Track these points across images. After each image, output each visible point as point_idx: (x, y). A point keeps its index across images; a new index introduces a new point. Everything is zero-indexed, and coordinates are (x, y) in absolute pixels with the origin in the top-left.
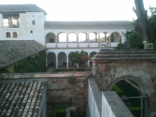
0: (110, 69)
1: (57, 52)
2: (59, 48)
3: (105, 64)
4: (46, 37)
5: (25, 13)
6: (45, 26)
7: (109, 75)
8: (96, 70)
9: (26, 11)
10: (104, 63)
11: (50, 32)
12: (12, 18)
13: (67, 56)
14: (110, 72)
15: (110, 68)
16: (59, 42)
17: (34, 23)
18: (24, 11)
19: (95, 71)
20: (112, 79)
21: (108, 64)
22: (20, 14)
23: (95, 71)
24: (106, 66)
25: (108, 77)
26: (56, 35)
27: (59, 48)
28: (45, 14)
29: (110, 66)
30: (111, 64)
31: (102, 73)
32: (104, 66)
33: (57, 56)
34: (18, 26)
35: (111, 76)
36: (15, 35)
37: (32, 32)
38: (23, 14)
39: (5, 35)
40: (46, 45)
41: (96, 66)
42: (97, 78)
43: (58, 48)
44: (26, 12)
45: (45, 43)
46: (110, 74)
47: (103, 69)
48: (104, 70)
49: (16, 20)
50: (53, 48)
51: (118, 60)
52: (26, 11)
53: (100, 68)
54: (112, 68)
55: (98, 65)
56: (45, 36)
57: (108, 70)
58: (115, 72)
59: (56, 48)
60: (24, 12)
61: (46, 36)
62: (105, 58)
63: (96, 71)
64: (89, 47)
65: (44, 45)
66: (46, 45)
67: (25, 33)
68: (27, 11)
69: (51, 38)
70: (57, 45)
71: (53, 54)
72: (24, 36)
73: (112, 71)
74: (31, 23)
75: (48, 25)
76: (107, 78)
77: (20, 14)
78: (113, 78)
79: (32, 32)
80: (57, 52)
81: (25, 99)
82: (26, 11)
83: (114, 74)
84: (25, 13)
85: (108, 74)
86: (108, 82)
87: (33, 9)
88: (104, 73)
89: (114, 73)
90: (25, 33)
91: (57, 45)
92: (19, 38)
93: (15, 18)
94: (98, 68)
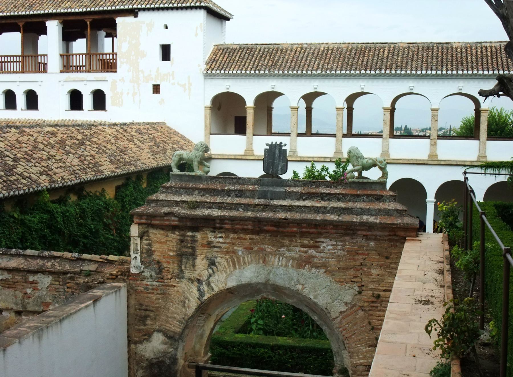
0: (193, 255)
3: (177, 233)
4: (209, 111)
5: (136, 15)
6: (207, 64)
8: (142, 253)
10: (173, 228)
12: (103, 33)
14: (194, 266)
15: (193, 249)
17: (166, 52)
18: (131, 7)
19: (136, 257)
20: (201, 293)
21: (189, 234)
22: (120, 21)
23: (138, 256)
24: (182, 241)
26: (250, 103)
29: (194, 240)
30: (199, 236)
32: (174, 236)
34: (109, 66)
35: (199, 281)
36: (99, 100)
37: (156, 89)
41: (141, 237)
42: (145, 282)
45: (206, 136)
46: (196, 275)
48: (171, 254)
51: (222, 219)
52: (139, 6)
55: (151, 235)
57: (186, 254)
58: (215, 268)
60: (133, 12)
61: (208, 104)
62: (176, 209)
63: (141, 256)
64: (432, 162)
68: (144, 9)
72: (129, 103)
73: (201, 262)
75: (225, 59)
76: (183, 285)
77: (120, 21)
79: (156, 89)
82: (140, 9)
84: (136, 16)
85: (187, 274)
89: (210, 271)
94: (150, 245)
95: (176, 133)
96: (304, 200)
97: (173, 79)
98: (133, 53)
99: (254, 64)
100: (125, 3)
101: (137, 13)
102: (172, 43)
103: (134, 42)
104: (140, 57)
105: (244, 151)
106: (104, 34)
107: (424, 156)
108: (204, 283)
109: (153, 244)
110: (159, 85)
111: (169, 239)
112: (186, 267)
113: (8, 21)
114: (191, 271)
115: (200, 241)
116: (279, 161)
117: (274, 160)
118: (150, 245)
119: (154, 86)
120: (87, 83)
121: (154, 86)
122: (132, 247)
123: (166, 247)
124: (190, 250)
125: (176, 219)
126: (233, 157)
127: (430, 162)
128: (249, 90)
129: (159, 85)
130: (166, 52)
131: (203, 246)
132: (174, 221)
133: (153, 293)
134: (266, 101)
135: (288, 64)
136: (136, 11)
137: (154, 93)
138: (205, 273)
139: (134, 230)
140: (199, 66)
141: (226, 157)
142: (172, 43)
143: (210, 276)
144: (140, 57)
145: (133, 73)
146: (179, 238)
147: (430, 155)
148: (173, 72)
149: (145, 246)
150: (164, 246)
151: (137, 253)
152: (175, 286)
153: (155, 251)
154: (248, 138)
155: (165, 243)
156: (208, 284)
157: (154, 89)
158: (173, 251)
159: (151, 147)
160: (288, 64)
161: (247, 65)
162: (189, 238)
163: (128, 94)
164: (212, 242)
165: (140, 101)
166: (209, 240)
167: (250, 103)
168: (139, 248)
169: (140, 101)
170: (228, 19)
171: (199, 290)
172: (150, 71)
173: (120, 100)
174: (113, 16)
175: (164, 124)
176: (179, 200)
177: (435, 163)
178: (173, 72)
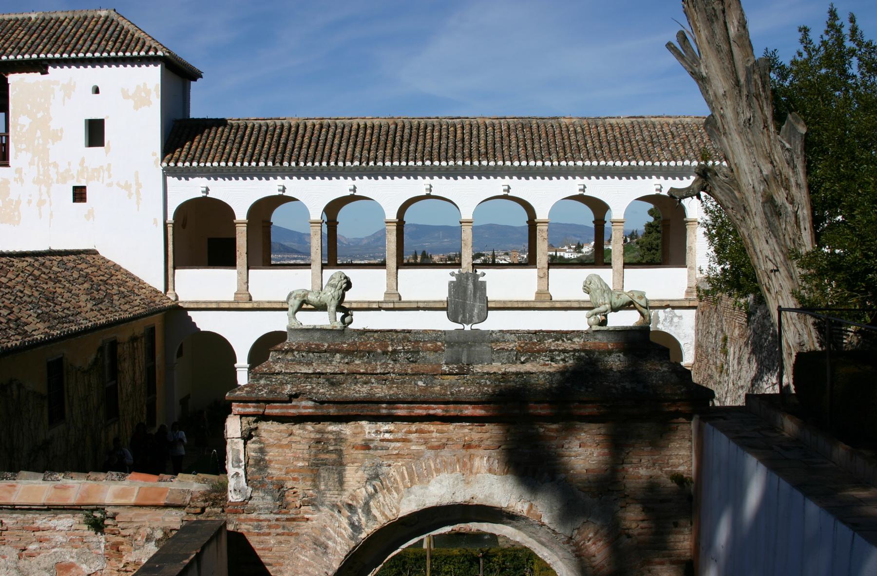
0: (339, 465)
5: (44, 72)
7: (338, 500)
11: (201, 195)
14: (341, 482)
15: (340, 453)
17: (95, 132)
19: (237, 474)
20: (356, 528)
23: (242, 472)
24: (318, 442)
25: (325, 509)
26: (241, 215)
29: (340, 439)
31: (289, 484)
37: (79, 194)
42: (253, 515)
44: (50, 69)
46: (345, 498)
47: (298, 459)
48: (300, 464)
53: (272, 454)
54: (350, 454)
55: (263, 434)
57: (327, 462)
58: (376, 483)
60: (40, 67)
67: (41, 203)
74: (81, 133)
78: (363, 520)
79: (79, 194)
83: (371, 496)
85: (331, 496)
86: (330, 543)
88: (302, 487)
90: (41, 203)
94: (262, 451)
95: (117, 268)
96: (522, 363)
97: (110, 177)
98: (39, 134)
99: (246, 151)
100: (23, 50)
102: (107, 117)
103: (39, 115)
104: (50, 141)
105: (233, 296)
107: (529, 294)
108: (360, 511)
109: (267, 449)
110: (84, 187)
111: (294, 438)
112: (326, 485)
114: (336, 492)
115: (351, 440)
116: (475, 301)
117: (465, 300)
118: (262, 451)
119: (75, 188)
121: (75, 188)
122: (230, 456)
123: (289, 454)
124: (334, 456)
125: (311, 403)
126: (214, 306)
127: (539, 305)
128: (240, 195)
129: (84, 187)
130: (95, 132)
131: (355, 447)
132: (305, 407)
133: (269, 534)
134: (263, 210)
135: (304, 151)
136: (46, 63)
137: (74, 201)
138: (362, 493)
139: (233, 427)
140: (154, 154)
141: (203, 306)
142: (107, 117)
143: (371, 496)
144: (50, 141)
145: (38, 166)
146: (313, 436)
147: (538, 293)
148: (109, 165)
149: (253, 454)
150: (287, 451)
151: (239, 467)
152: (308, 519)
153: (271, 461)
154: (239, 273)
155: (289, 446)
156: (367, 510)
157: (74, 194)
158: (304, 460)
159: (88, 292)
160: (304, 151)
161: (234, 152)
162: (331, 436)
163: (30, 202)
164: (372, 440)
165: (51, 215)
166: (367, 436)
167: (241, 215)
168: (242, 457)
169: (51, 215)
170: (195, 80)
171: (352, 525)
172: (69, 164)
173: (16, 213)
175: (95, 253)
176: (310, 371)
177: (547, 305)
178: (109, 165)
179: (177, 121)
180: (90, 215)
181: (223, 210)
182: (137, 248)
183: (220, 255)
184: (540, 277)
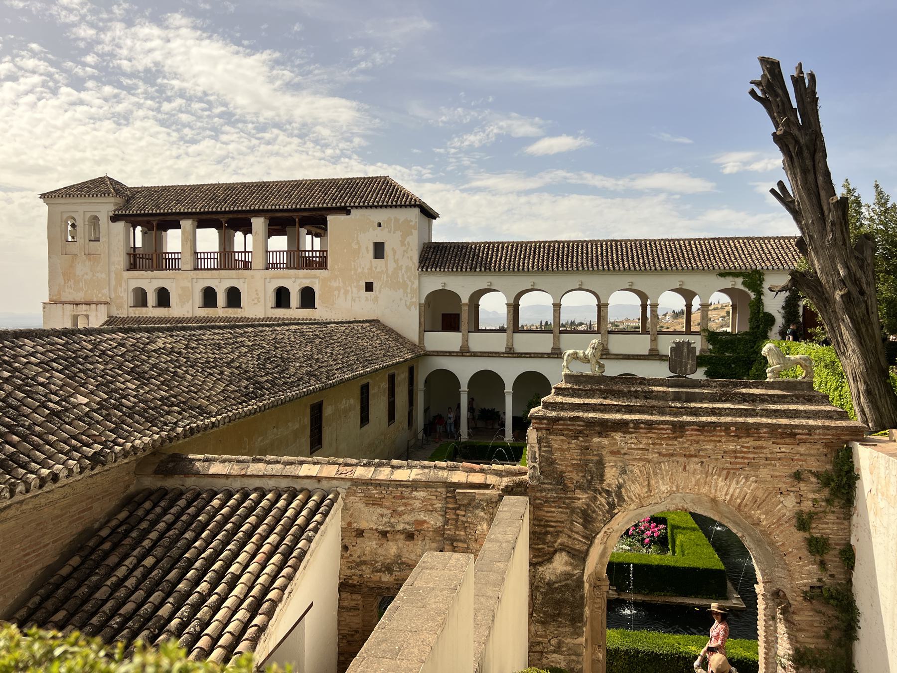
1: (464, 371)
2: (475, 355)
5: (348, 213)
9: (352, 207)
12: (303, 231)
13: (509, 389)
16: (482, 326)
17: (379, 250)
22: (330, 218)
26: (465, 300)
27: (475, 355)
28: (429, 214)
33: (464, 387)
36: (308, 297)
37: (369, 287)
38: (342, 218)
39: (271, 299)
40: (421, 338)
43: (469, 352)
49: (317, 241)
50: (450, 354)
56: (420, 305)
59: (465, 352)
60: (346, 210)
61: (423, 301)
65: (416, 339)
66: (421, 338)
69: (447, 314)
70: (466, 340)
71: (449, 378)
72: (341, 301)
75: (436, 256)
79: (369, 287)
80: (464, 371)
81: (243, 557)
84: (348, 213)
87: (383, 195)
91: (466, 340)
92: (320, 312)
93: (314, 230)
101: (349, 211)
106: (306, 231)
113: (209, 216)
120: (294, 282)
130: (379, 250)
167: (465, 300)
174: (323, 213)
179: (424, 244)
180: (376, 299)
181: (454, 297)
182: (406, 320)
183: (450, 323)
184: (652, 340)
